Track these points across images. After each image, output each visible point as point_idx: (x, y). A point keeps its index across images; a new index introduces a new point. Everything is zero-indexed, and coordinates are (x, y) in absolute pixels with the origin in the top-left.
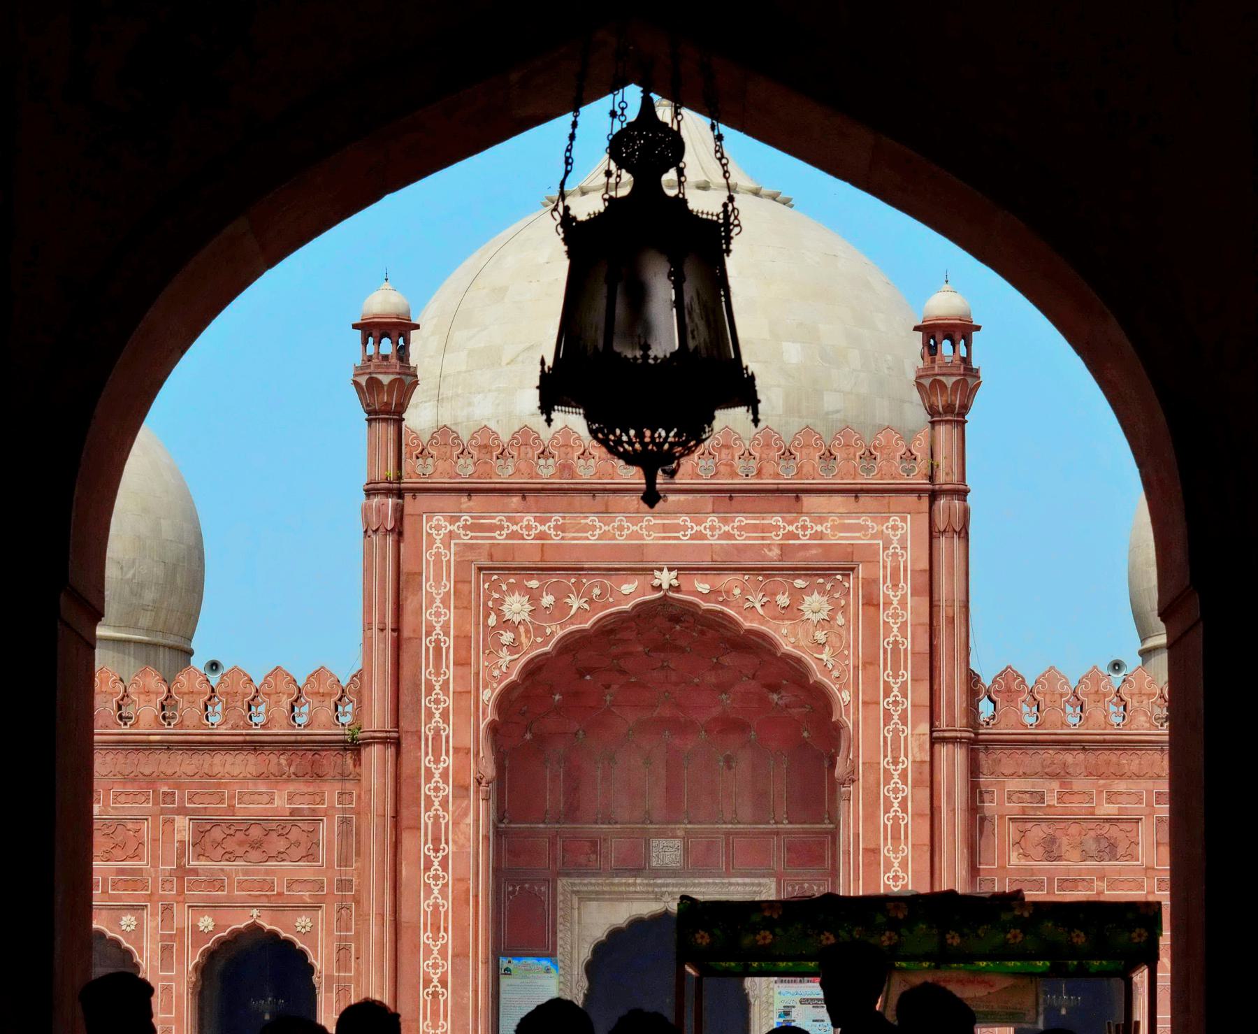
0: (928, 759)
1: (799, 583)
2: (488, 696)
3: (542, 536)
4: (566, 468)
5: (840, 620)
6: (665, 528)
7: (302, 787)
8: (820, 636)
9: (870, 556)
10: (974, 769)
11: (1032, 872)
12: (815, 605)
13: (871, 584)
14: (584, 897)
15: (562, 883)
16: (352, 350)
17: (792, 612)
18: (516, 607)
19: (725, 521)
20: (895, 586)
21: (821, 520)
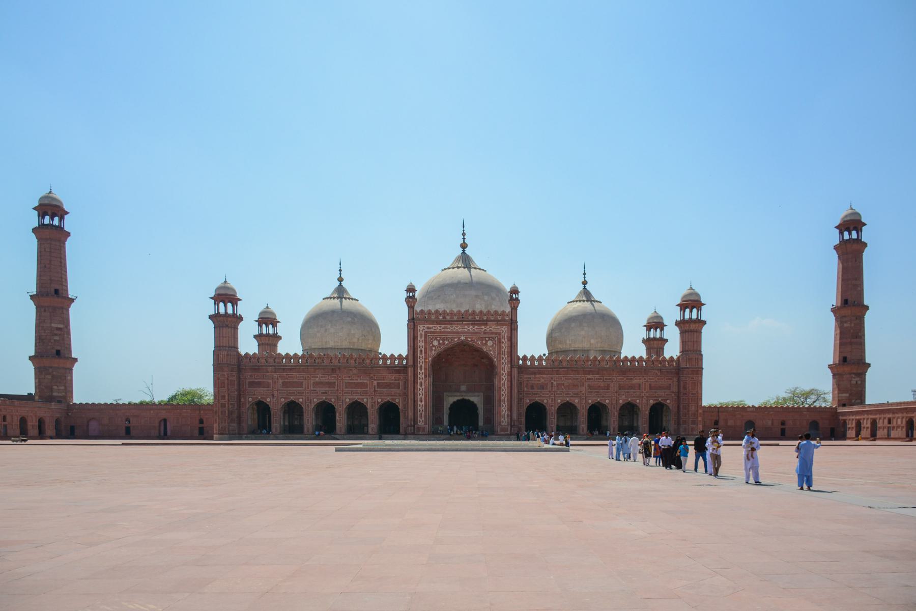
4: (444, 317)
7: (397, 375)
9: (500, 334)
10: (519, 373)
12: (490, 343)
13: (500, 339)
17: (486, 344)
18: (435, 343)
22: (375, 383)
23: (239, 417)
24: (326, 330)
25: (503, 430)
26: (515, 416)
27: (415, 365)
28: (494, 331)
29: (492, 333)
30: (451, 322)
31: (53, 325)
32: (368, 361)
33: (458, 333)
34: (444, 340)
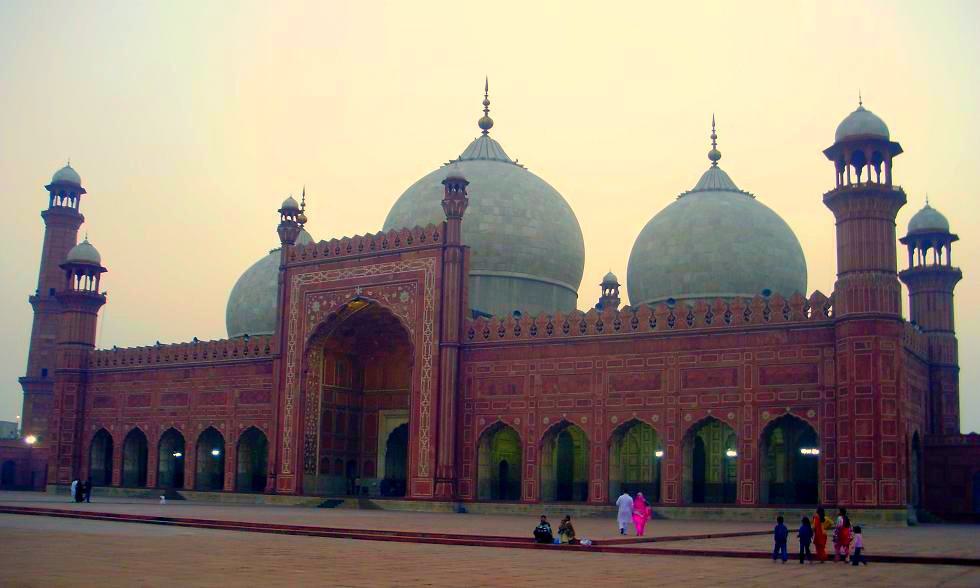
0: (437, 354)
1: (400, 288)
2: (306, 339)
3: (324, 279)
5: (412, 301)
6: (360, 272)
8: (405, 308)
11: (483, 400)
12: (404, 296)
13: (422, 286)
14: (387, 417)
15: (380, 412)
16: (278, 219)
17: (397, 300)
18: (316, 306)
19: (377, 267)
20: (430, 286)
21: (406, 263)
22: (237, 391)
23: (78, 459)
24: (238, 305)
25: (423, 488)
26: (446, 457)
27: (281, 356)
28: (414, 269)
29: (408, 275)
30: (340, 263)
31: (44, 336)
32: (230, 353)
33: (350, 282)
34: (328, 300)
